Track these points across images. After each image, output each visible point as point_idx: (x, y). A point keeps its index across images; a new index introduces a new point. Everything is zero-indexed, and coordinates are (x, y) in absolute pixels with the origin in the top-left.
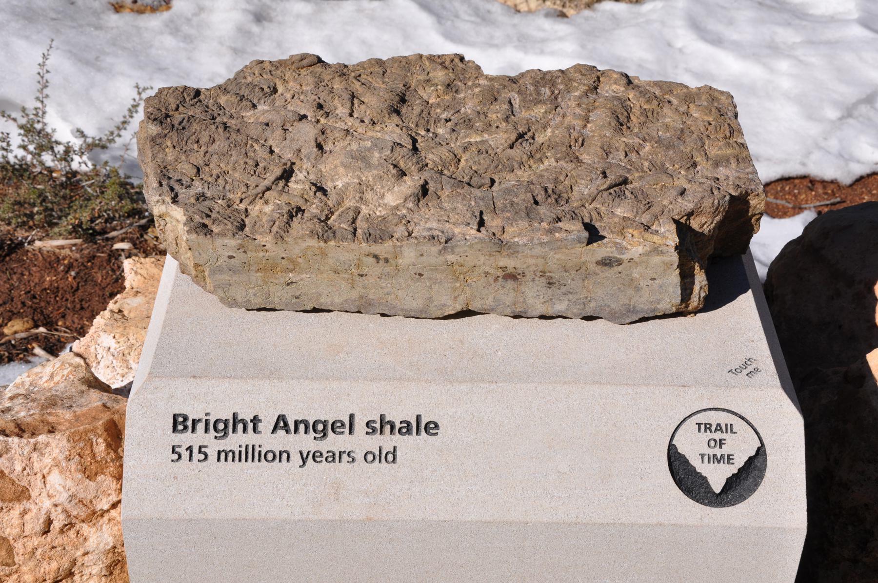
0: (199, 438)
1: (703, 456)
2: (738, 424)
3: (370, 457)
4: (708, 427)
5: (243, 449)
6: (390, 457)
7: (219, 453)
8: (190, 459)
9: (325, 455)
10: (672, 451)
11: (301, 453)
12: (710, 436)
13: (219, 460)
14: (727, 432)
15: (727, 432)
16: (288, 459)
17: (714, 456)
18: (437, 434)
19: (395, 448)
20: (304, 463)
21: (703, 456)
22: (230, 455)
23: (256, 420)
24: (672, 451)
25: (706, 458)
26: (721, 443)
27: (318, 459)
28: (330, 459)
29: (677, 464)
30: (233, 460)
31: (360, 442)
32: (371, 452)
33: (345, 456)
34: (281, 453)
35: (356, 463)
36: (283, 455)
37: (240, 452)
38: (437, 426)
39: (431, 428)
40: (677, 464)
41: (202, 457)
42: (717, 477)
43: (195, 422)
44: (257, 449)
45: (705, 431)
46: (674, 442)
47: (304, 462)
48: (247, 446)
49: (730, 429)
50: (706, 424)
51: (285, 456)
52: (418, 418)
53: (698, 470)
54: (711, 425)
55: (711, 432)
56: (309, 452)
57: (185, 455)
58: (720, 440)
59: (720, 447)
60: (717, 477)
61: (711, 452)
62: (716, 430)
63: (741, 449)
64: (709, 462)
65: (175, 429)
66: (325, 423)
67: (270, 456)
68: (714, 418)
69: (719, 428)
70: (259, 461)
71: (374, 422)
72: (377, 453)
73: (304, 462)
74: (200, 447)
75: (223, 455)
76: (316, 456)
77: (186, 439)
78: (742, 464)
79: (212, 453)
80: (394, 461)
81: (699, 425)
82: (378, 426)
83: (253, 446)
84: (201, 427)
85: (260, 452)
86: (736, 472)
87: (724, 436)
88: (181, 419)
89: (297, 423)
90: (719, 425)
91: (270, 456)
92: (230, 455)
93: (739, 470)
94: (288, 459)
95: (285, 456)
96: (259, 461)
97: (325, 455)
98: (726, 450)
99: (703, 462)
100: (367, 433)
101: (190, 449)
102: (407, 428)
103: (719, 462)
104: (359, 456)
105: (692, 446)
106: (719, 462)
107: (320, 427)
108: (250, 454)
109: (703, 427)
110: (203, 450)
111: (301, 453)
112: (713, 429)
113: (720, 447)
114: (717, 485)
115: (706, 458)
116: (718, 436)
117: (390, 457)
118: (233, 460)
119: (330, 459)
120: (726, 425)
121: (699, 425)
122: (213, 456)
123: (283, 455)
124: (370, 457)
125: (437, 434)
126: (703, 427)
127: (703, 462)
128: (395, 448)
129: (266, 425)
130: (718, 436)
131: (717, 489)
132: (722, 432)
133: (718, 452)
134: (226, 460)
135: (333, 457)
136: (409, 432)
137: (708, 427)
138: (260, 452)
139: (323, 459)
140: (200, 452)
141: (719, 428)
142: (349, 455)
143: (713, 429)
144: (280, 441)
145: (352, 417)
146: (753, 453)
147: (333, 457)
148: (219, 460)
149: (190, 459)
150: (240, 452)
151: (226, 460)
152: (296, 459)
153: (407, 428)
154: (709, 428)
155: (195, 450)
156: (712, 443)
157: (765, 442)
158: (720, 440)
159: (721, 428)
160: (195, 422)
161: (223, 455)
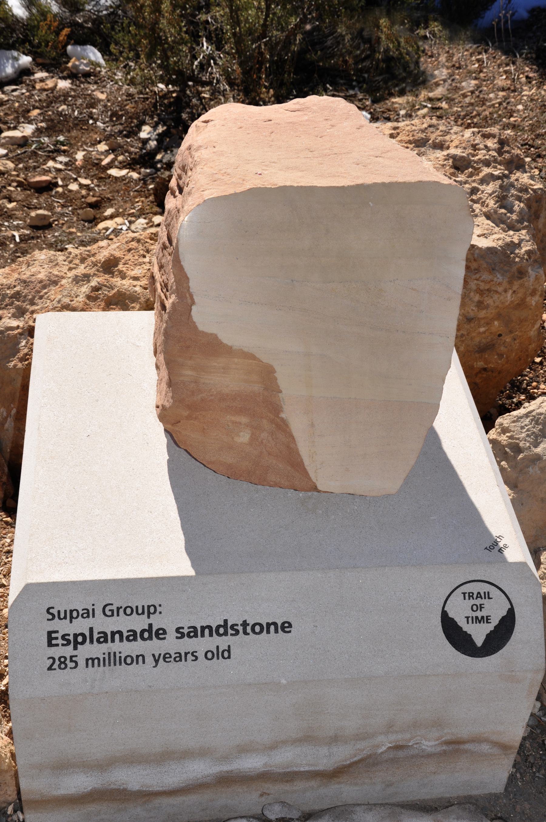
1: (467, 618)
3: (210, 655)
6: (226, 654)
7: (87, 660)
9: (173, 656)
11: (154, 655)
12: (472, 602)
14: (485, 598)
15: (485, 598)
16: (144, 662)
17: (477, 618)
19: (229, 646)
21: (467, 618)
22: (96, 661)
25: (470, 619)
26: (481, 607)
27: (167, 660)
28: (178, 659)
33: (189, 656)
41: (73, 665)
44: (118, 655)
45: (469, 599)
47: (157, 661)
48: (109, 653)
49: (488, 596)
50: (469, 593)
51: (140, 658)
53: (464, 629)
54: (473, 594)
55: (473, 599)
56: (160, 655)
58: (481, 605)
59: (481, 610)
61: (474, 614)
62: (477, 597)
64: (473, 623)
67: (129, 660)
69: (479, 595)
73: (157, 661)
76: (166, 657)
80: (229, 657)
81: (464, 594)
85: (120, 657)
90: (479, 593)
91: (129, 660)
92: (96, 661)
94: (144, 662)
95: (140, 658)
97: (173, 656)
98: (484, 613)
99: (468, 623)
103: (480, 622)
104: (201, 655)
105: (459, 611)
106: (480, 622)
108: (113, 659)
110: (74, 659)
111: (154, 655)
112: (475, 596)
113: (481, 610)
115: (470, 619)
116: (478, 602)
117: (226, 654)
118: (99, 665)
119: (178, 659)
120: (485, 593)
121: (464, 594)
122: (82, 663)
124: (210, 655)
127: (468, 623)
128: (229, 646)
130: (478, 602)
132: (482, 599)
133: (479, 614)
134: (93, 666)
138: (120, 657)
139: (172, 659)
140: (71, 661)
141: (479, 595)
143: (475, 596)
150: (104, 658)
151: (93, 666)
152: (150, 660)
158: (481, 605)
159: (481, 597)
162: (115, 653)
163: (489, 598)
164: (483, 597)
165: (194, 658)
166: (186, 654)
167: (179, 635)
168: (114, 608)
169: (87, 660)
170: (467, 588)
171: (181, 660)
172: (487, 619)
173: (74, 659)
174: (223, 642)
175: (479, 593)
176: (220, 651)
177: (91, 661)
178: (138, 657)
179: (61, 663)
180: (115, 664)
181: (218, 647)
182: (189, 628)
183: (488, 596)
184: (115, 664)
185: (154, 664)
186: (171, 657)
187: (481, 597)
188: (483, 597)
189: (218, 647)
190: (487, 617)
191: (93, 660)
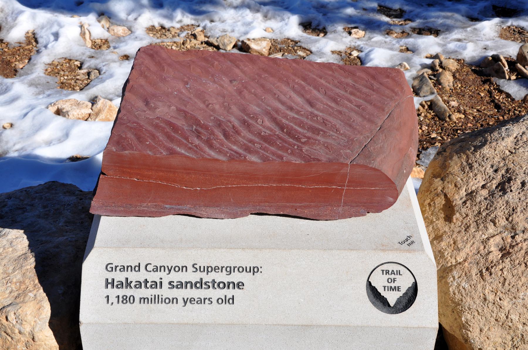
1: (385, 287)
3: (220, 301)
4: (387, 272)
5: (153, 297)
6: (231, 301)
12: (388, 276)
17: (391, 287)
21: (385, 287)
22: (146, 300)
25: (386, 288)
27: (192, 302)
29: (374, 293)
30: (148, 303)
33: (206, 301)
34: (173, 299)
36: (174, 300)
40: (374, 293)
42: (392, 298)
46: (369, 280)
47: (185, 303)
51: (175, 300)
58: (394, 279)
60: (392, 298)
61: (389, 285)
63: (405, 283)
67: (167, 301)
73: (185, 303)
75: (142, 300)
76: (192, 300)
81: (383, 271)
83: (159, 295)
86: (401, 295)
90: (393, 271)
91: (167, 301)
92: (146, 300)
95: (175, 300)
98: (396, 284)
103: (393, 290)
104: (214, 301)
105: (379, 282)
106: (393, 290)
108: (156, 299)
109: (385, 272)
115: (386, 288)
116: (393, 276)
117: (231, 301)
118: (148, 303)
119: (199, 302)
121: (383, 271)
123: (174, 300)
124: (220, 301)
126: (385, 272)
127: (385, 290)
128: (233, 296)
133: (393, 285)
135: (201, 301)
137: (387, 272)
139: (195, 302)
142: (209, 300)
143: (390, 273)
146: (410, 285)
147: (201, 301)
152: (181, 301)
156: (390, 281)
158: (394, 279)
161: (142, 300)
162: (159, 295)
163: (400, 274)
164: (396, 273)
165: (209, 302)
166: (205, 299)
167: (170, 287)
168: (113, 266)
169: (141, 299)
170: (385, 267)
174: (229, 293)
175: (393, 271)
177: (143, 300)
178: (173, 299)
179: (124, 299)
181: (226, 296)
182: (177, 282)
185: (183, 304)
188: (396, 273)
189: (226, 296)
190: (398, 287)
191: (145, 299)
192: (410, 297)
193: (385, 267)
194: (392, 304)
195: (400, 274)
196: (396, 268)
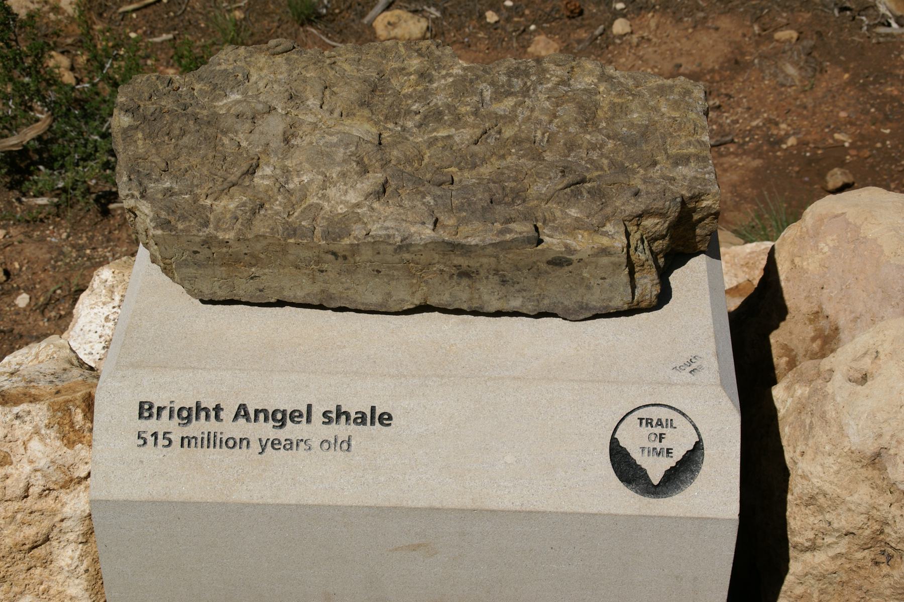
0: (163, 424)
1: (643, 449)
2: (678, 419)
3: (326, 445)
4: (649, 422)
5: (206, 436)
6: (345, 446)
7: (183, 439)
8: (156, 444)
9: (283, 443)
10: (614, 442)
11: (260, 440)
13: (182, 446)
18: (390, 424)
20: (263, 450)
21: (643, 449)
23: (218, 409)
24: (614, 442)
26: (661, 437)
27: (277, 447)
31: (317, 430)
32: (327, 441)
33: (302, 444)
35: (312, 451)
36: (244, 442)
37: (202, 438)
38: (390, 418)
39: (385, 419)
42: (656, 469)
43: (160, 409)
44: (219, 436)
46: (616, 436)
48: (209, 433)
49: (670, 423)
50: (647, 419)
51: (245, 442)
52: (373, 409)
53: (638, 463)
57: (151, 440)
58: (661, 434)
59: (660, 441)
60: (656, 469)
62: (657, 424)
63: (680, 443)
65: (141, 416)
66: (284, 412)
67: (231, 443)
68: (655, 413)
69: (659, 423)
70: (221, 447)
71: (330, 412)
72: (333, 441)
74: (165, 433)
75: (186, 441)
76: (275, 444)
77: (151, 425)
78: (680, 458)
79: (176, 438)
80: (348, 450)
82: (334, 416)
84: (165, 414)
86: (674, 465)
87: (664, 431)
88: (146, 407)
89: (257, 412)
90: (659, 420)
91: (231, 443)
93: (677, 463)
95: (245, 442)
96: (221, 447)
98: (666, 444)
100: (324, 423)
101: (155, 435)
102: (361, 419)
104: (315, 443)
105: (634, 440)
107: (279, 416)
108: (210, 441)
109: (644, 421)
110: (168, 436)
111: (260, 440)
113: (660, 441)
114: (656, 477)
115: (646, 450)
116: (658, 430)
119: (288, 447)
120: (667, 420)
121: (641, 419)
123: (244, 442)
125: (390, 424)
126: (644, 421)
129: (228, 414)
131: (656, 482)
132: (663, 427)
133: (658, 446)
135: (290, 445)
136: (364, 422)
137: (649, 422)
139: (282, 447)
141: (659, 423)
143: (654, 423)
144: (241, 429)
145: (309, 407)
146: (691, 448)
147: (290, 445)
148: (182, 446)
149: (156, 444)
150: (202, 438)
152: (256, 447)
153: (361, 419)
154: (651, 423)
155: (160, 437)
156: (653, 437)
157: (703, 437)
159: (661, 425)
160: (160, 409)
161: (186, 441)
170: (644, 413)
171: (291, 448)
172: (668, 453)
173: (168, 436)
175: (659, 420)
176: (339, 442)
180: (215, 446)
183: (670, 423)
184: (215, 446)
186: (280, 443)
187: (661, 425)
190: (668, 449)
192: (687, 466)
193: (644, 413)
194: (656, 482)
195: (671, 425)
196: (663, 414)
